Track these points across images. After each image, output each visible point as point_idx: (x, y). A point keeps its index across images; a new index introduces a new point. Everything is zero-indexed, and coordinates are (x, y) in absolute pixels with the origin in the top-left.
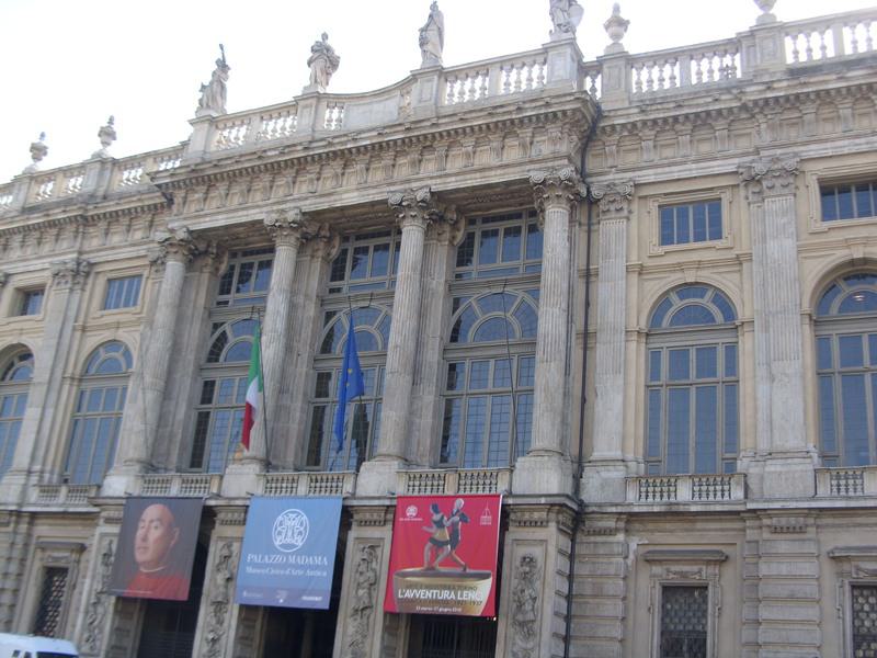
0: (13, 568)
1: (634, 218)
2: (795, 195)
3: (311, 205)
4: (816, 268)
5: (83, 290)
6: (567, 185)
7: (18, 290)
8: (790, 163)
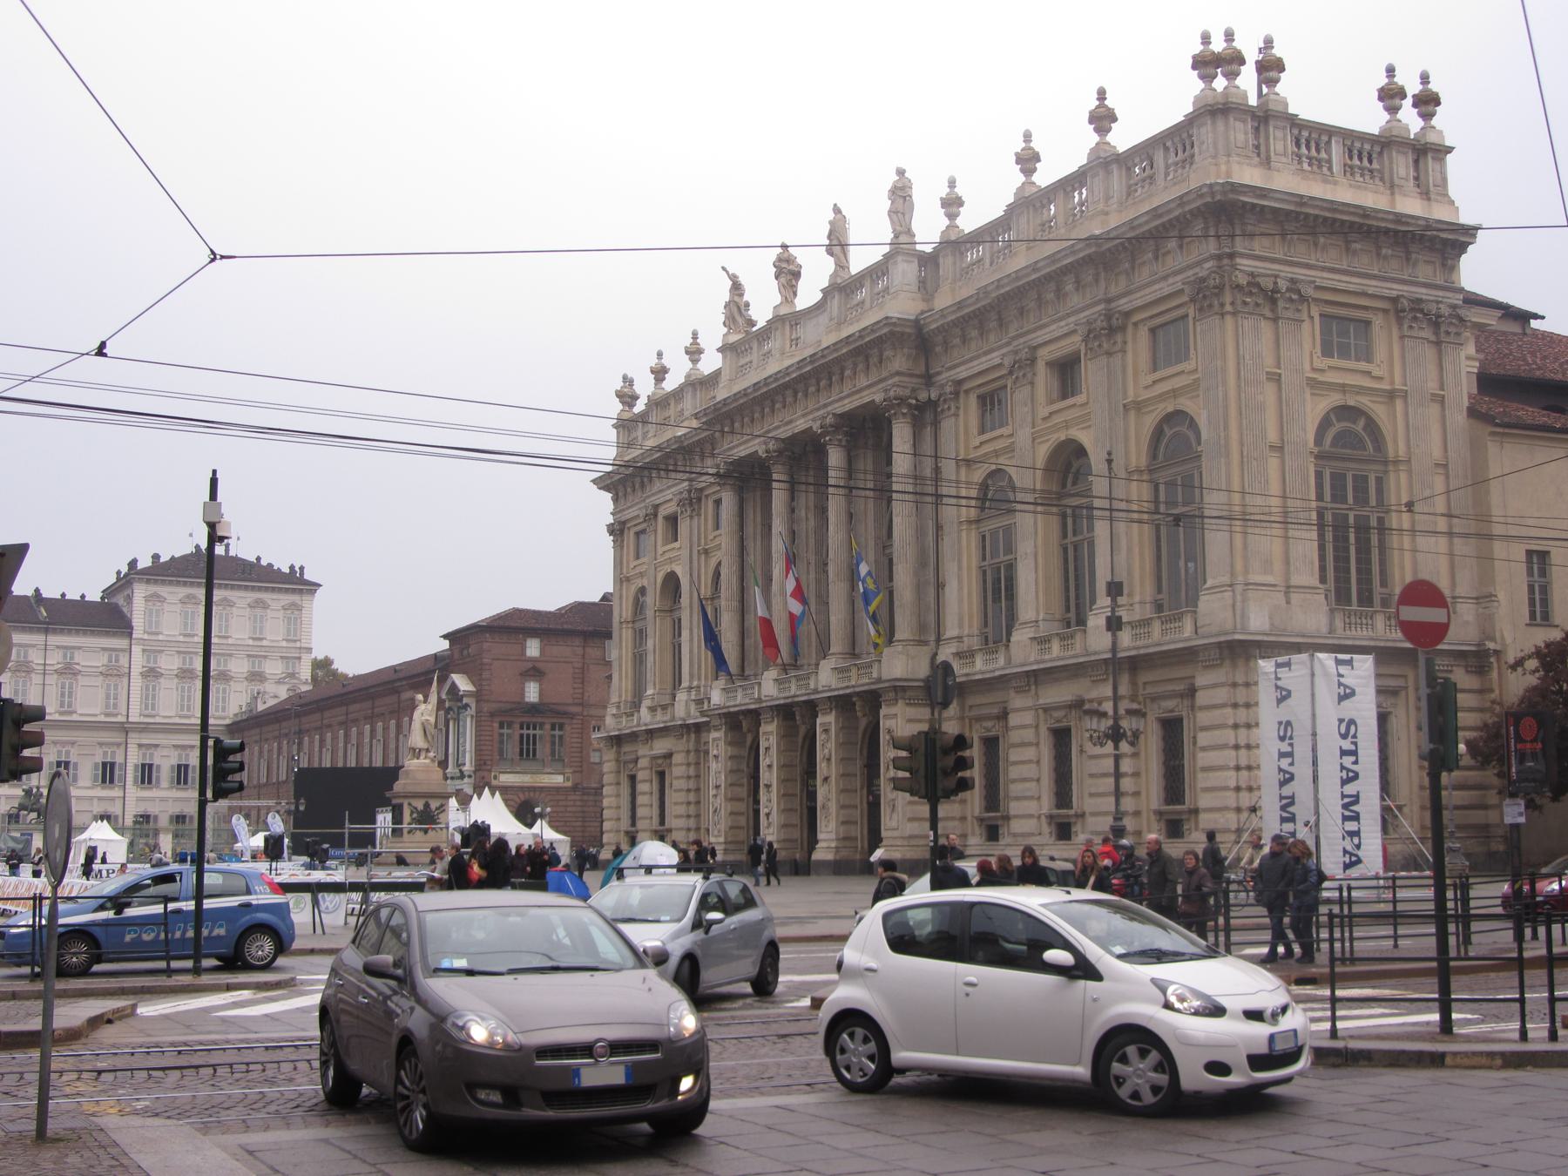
0: (692, 771)
1: (961, 412)
2: (1032, 383)
3: (784, 433)
4: (1043, 451)
5: (699, 515)
6: (902, 400)
7: (666, 518)
8: (1023, 355)
